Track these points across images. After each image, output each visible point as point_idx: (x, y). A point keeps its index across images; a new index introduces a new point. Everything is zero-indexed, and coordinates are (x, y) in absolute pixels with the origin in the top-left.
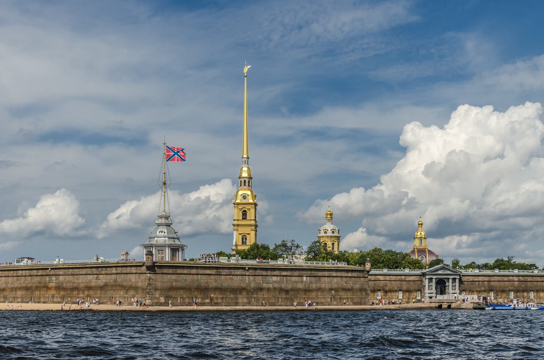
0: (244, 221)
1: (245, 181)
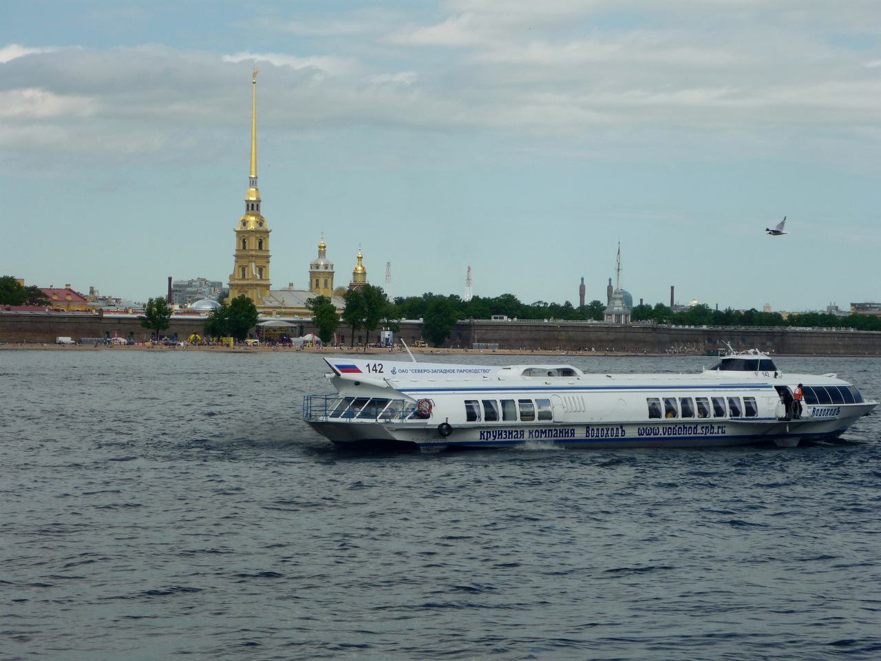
1: (257, 205)
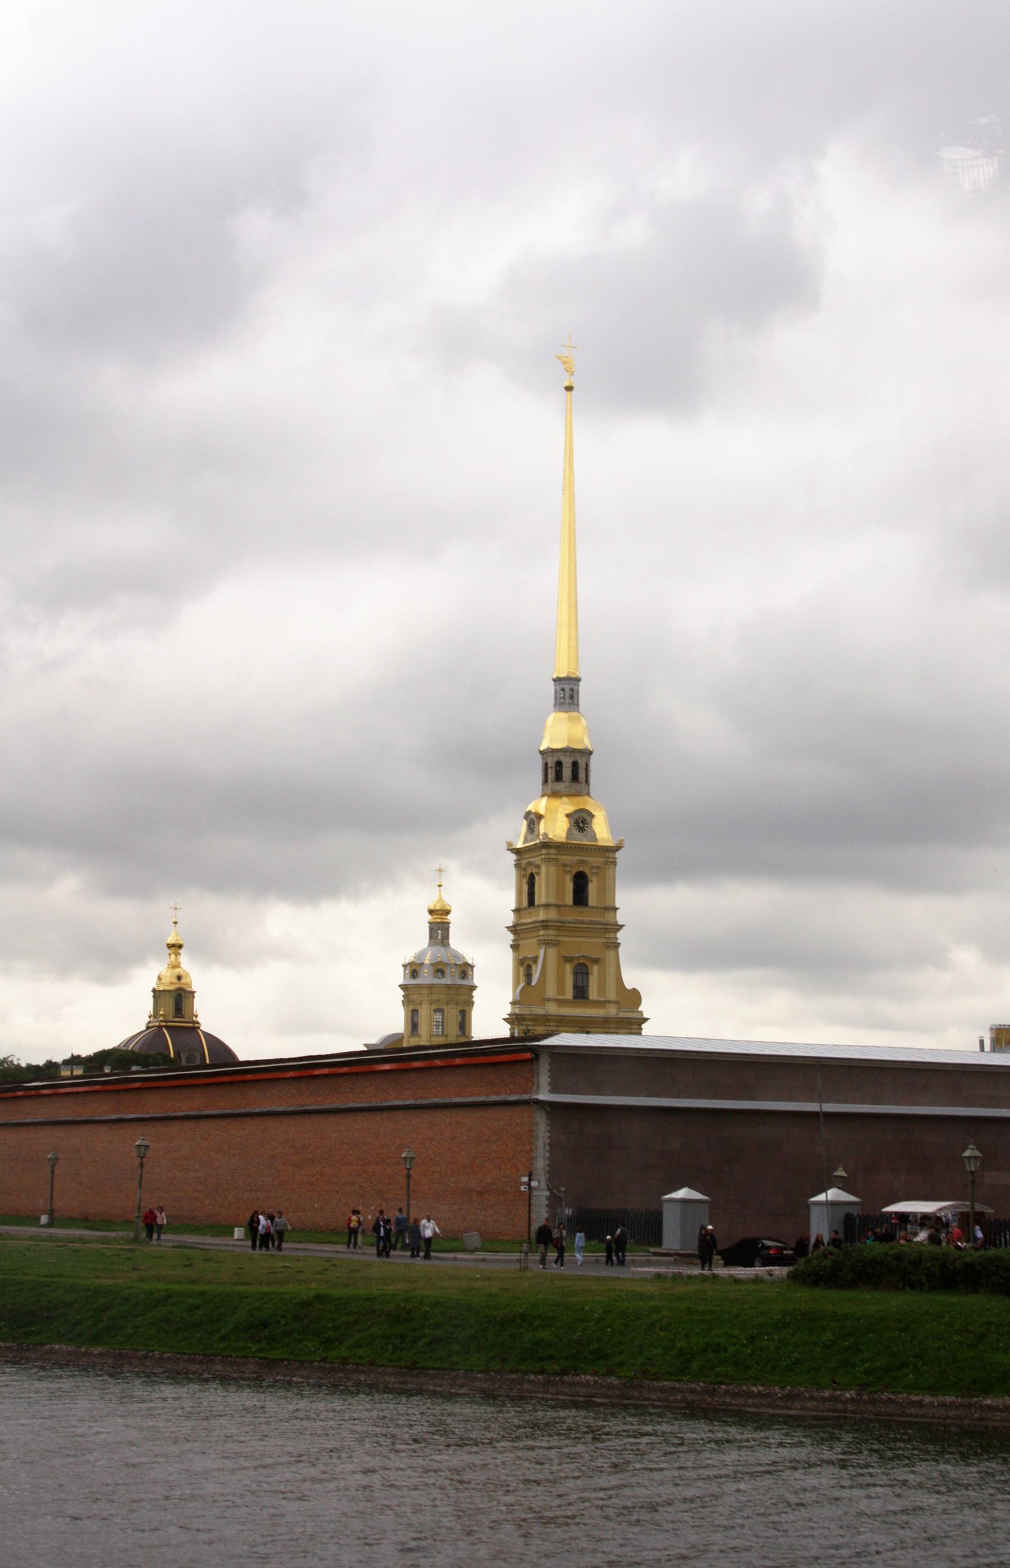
0: (582, 909)
1: (575, 765)
